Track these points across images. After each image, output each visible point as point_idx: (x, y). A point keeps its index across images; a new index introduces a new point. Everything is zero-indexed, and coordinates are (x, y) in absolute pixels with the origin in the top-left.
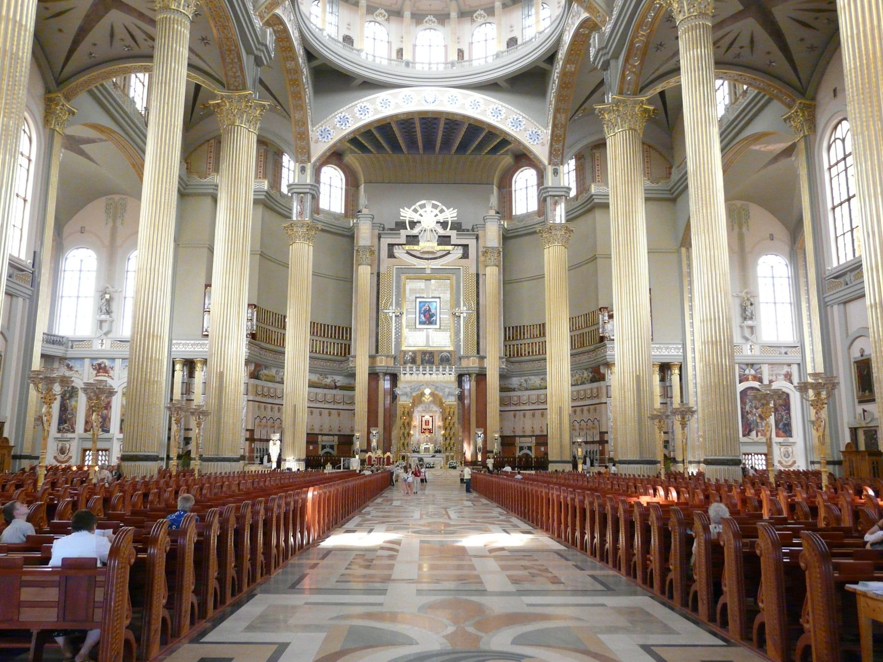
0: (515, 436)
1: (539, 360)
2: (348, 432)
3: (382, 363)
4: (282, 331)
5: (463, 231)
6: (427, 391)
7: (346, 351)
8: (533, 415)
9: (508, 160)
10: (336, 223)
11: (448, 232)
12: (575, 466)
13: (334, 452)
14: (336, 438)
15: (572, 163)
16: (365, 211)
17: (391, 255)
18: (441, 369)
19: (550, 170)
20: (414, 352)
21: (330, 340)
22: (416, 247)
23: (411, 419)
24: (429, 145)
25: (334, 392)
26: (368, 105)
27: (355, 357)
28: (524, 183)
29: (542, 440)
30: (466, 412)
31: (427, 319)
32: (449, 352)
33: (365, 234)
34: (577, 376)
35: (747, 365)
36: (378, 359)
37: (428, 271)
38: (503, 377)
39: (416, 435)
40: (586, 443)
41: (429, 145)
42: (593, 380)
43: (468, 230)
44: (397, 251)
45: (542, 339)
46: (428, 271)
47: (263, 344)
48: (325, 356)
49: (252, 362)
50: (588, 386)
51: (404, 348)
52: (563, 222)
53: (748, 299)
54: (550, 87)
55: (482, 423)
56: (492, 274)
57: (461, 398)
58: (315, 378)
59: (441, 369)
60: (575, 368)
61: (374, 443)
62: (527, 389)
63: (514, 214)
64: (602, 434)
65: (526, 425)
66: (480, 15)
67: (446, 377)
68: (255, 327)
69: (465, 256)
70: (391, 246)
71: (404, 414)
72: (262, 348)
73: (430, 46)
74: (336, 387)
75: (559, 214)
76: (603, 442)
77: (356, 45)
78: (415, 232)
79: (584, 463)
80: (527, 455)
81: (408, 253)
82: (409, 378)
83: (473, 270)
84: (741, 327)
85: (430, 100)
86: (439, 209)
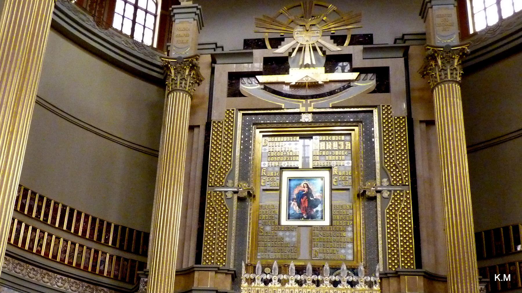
17: (234, 92)
63: (471, 32)
78: (282, 50)
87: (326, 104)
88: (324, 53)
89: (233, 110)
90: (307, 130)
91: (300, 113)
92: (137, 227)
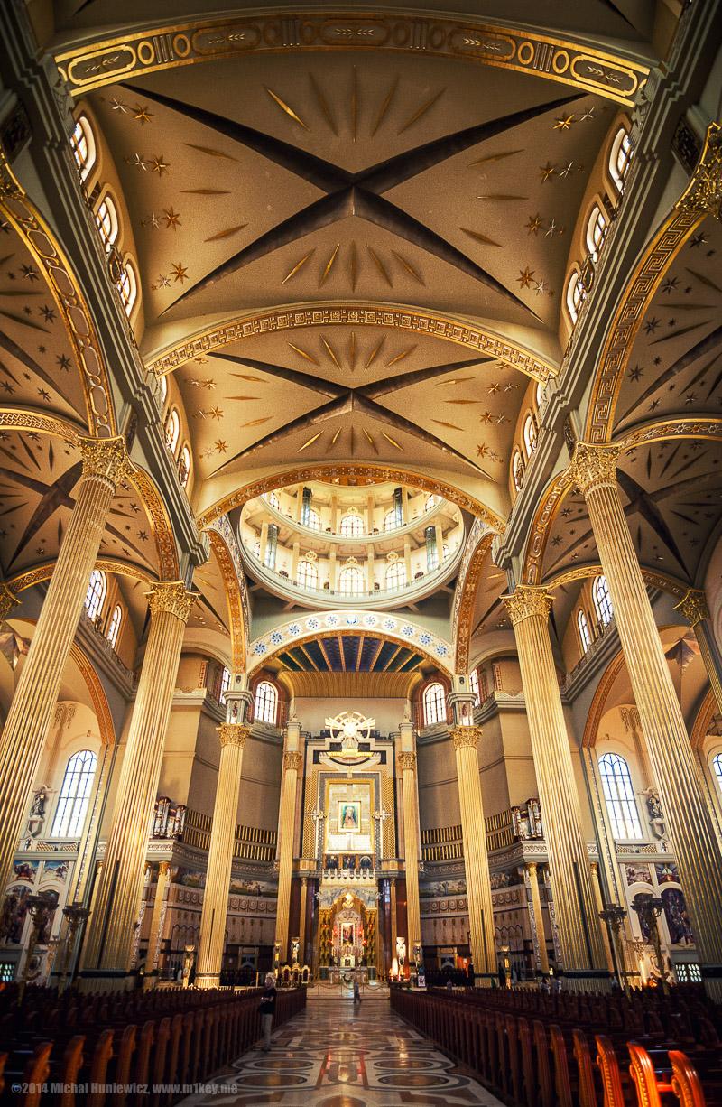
0: (436, 947)
1: (456, 868)
2: (270, 944)
3: (306, 867)
4: (208, 833)
5: (381, 738)
6: (349, 897)
7: (272, 856)
8: (454, 923)
9: (418, 676)
10: (268, 732)
11: (368, 740)
12: (503, 982)
13: (254, 966)
14: (257, 949)
15: (474, 675)
16: (294, 720)
17: (316, 761)
18: (361, 872)
19: (457, 678)
20: (337, 856)
21: (256, 844)
22: (338, 754)
23: (332, 928)
24: (351, 663)
25: (258, 899)
26: (298, 625)
27: (279, 861)
28: (434, 692)
29: (465, 951)
30: (387, 920)
31: (350, 826)
32: (369, 856)
33: (292, 741)
34: (495, 879)
35: (663, 864)
36: (301, 862)
37: (350, 776)
38: (423, 880)
39: (337, 944)
40: (513, 953)
41: (351, 663)
42: (511, 883)
43: (385, 738)
44: (322, 758)
45: (459, 842)
46: (350, 776)
47: (190, 848)
48: (252, 861)
49: (175, 865)
50: (506, 890)
51: (327, 852)
52: (472, 723)
53: (653, 797)
54: (453, 608)
55: (403, 932)
56: (408, 779)
57: (381, 903)
58: (238, 883)
59: (361, 872)
60: (493, 870)
61: (295, 955)
62: (445, 895)
64: (527, 942)
65: (449, 934)
66: (392, 555)
67: (367, 882)
68: (182, 829)
69: (383, 761)
70: (316, 753)
71: (324, 921)
72: (187, 851)
73: (352, 581)
74: (260, 894)
75: (467, 721)
76: (528, 952)
77: (290, 577)
78: (338, 740)
79: (512, 978)
80: (449, 967)
81: (331, 759)
82: (329, 881)
83: (391, 775)
84: (652, 825)
85: (352, 620)
86: (359, 719)
87: (358, 770)
92: (268, 828)
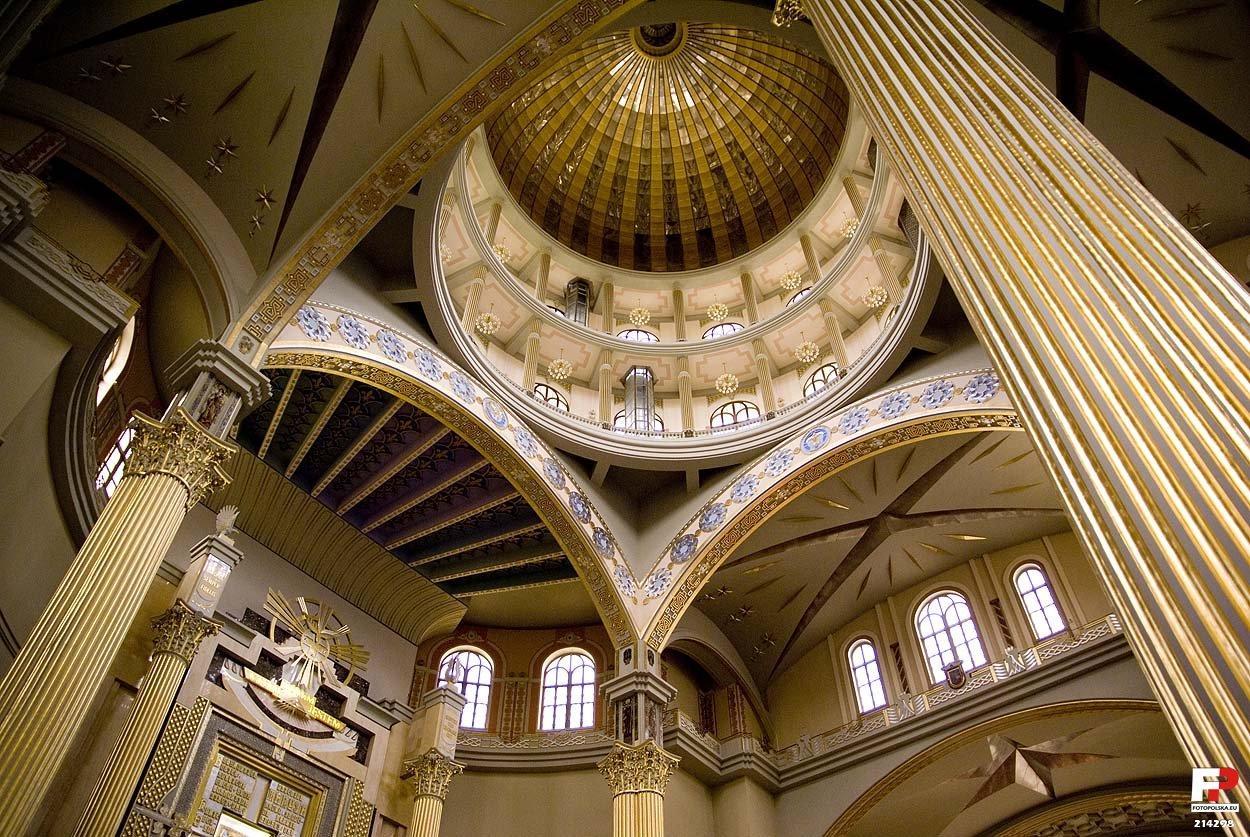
11: (344, 690)
22: (270, 684)
44: (227, 672)
69: (361, 756)
70: (222, 653)
78: (284, 650)
81: (248, 689)
87: (303, 747)
88: (323, 679)
89: (206, 701)
90: (268, 769)
91: (274, 744)
